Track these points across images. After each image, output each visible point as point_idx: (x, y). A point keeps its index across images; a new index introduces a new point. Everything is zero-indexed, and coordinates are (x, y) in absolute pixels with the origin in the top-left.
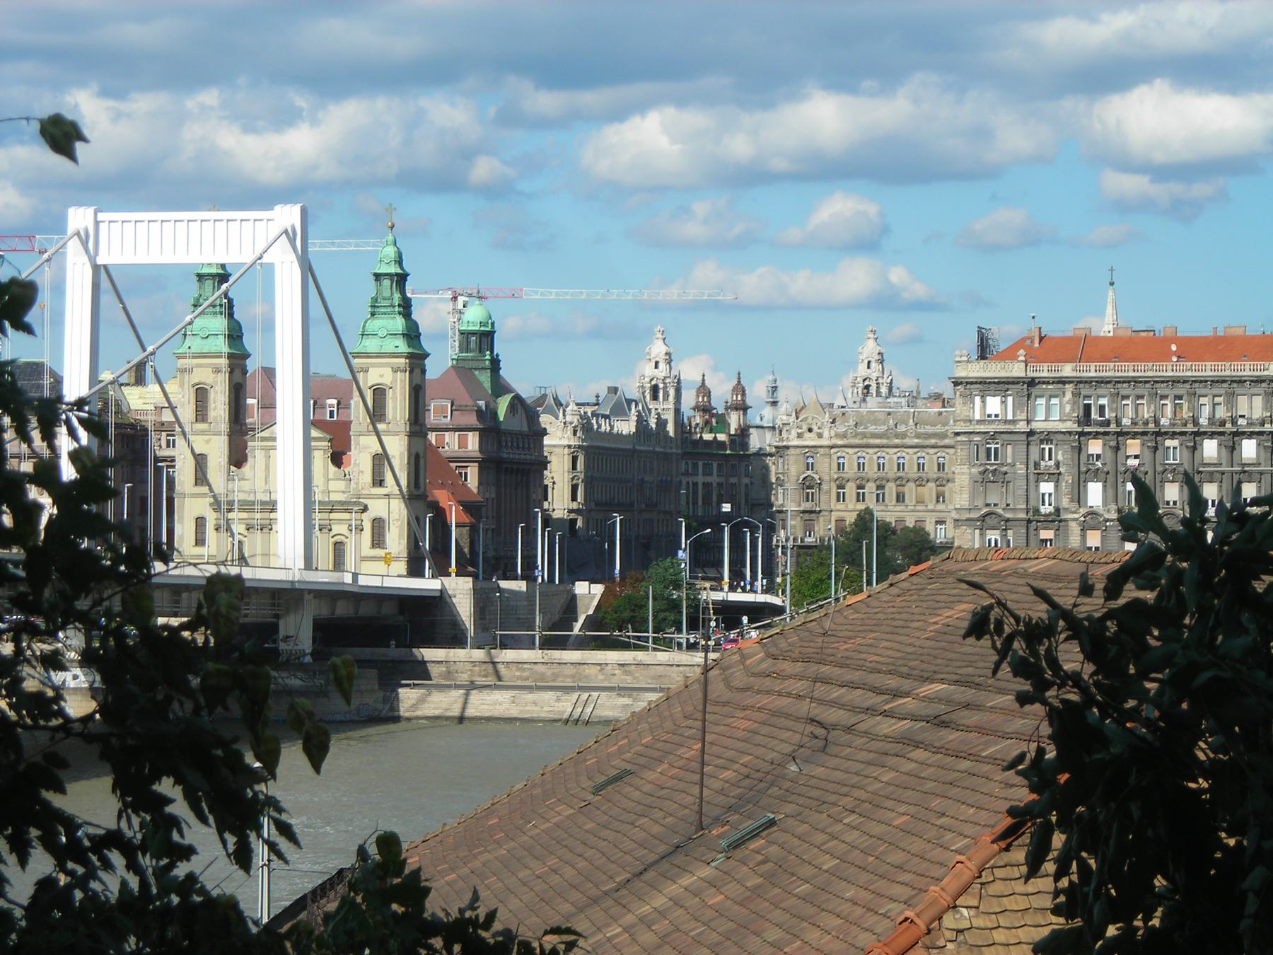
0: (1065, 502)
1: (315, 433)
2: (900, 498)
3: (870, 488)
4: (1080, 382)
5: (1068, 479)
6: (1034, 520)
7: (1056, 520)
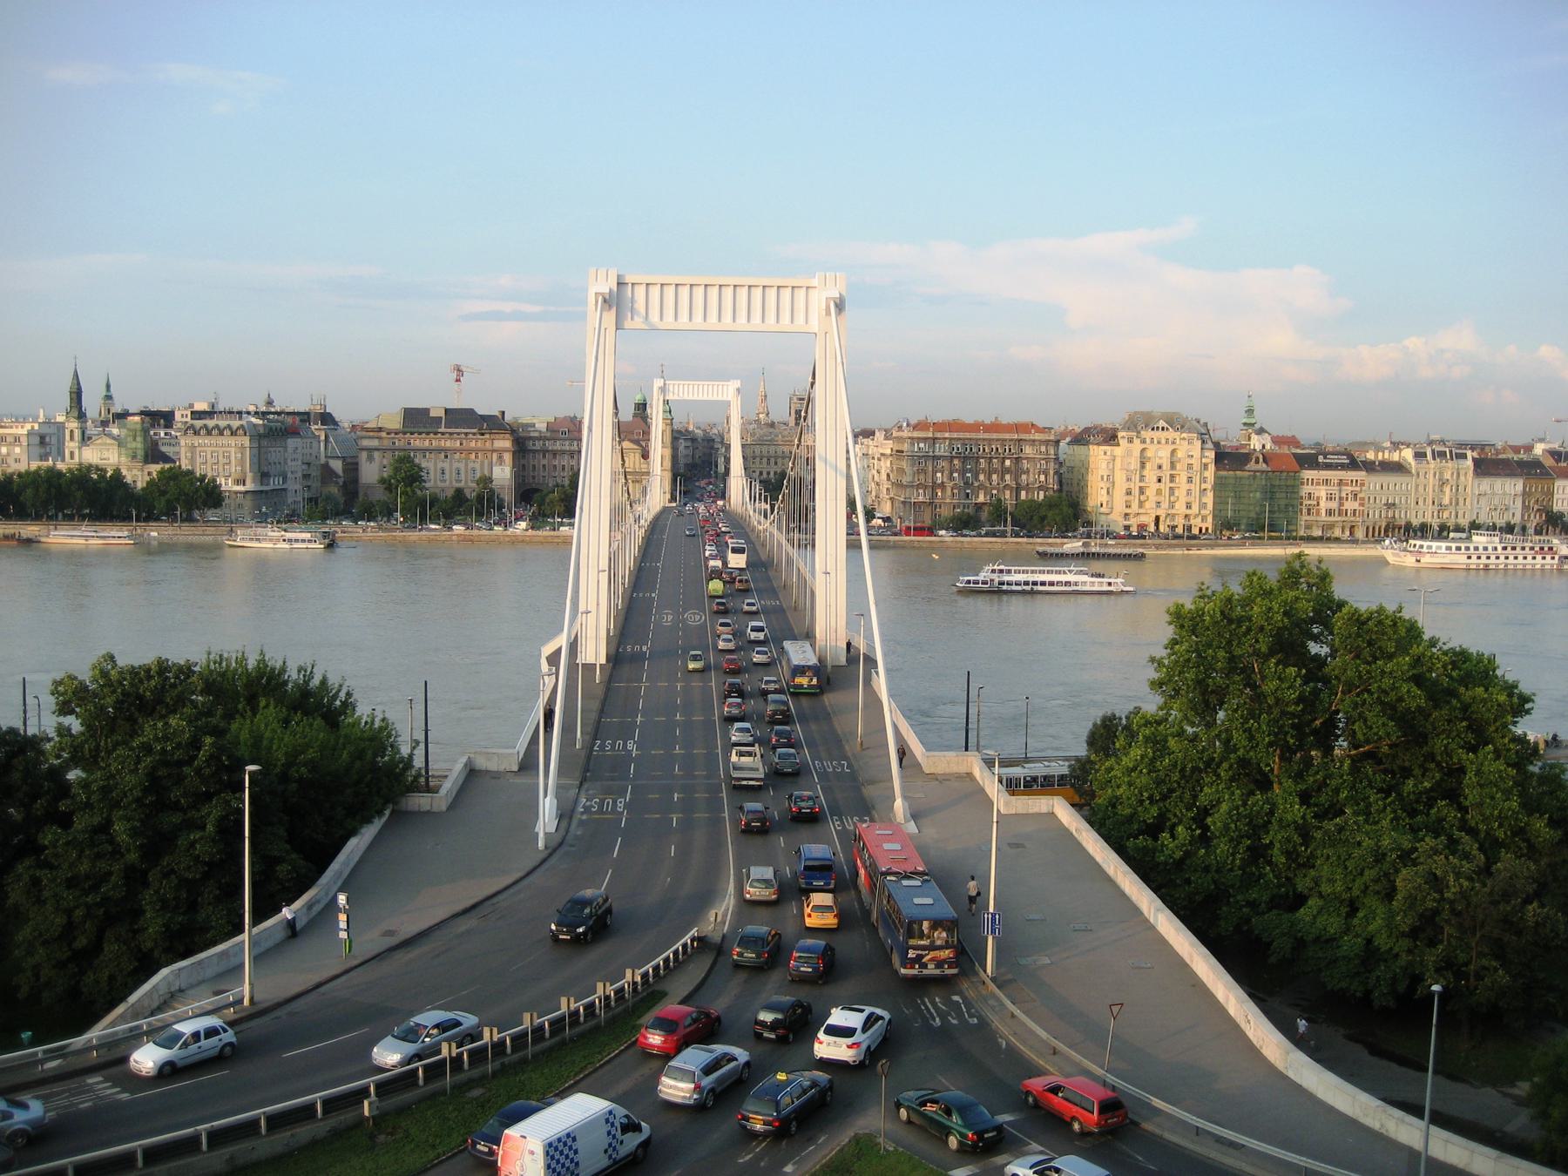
0: (945, 480)
1: (626, 444)
2: (776, 463)
3: (765, 460)
4: (951, 439)
5: (946, 472)
6: (934, 486)
7: (942, 486)
